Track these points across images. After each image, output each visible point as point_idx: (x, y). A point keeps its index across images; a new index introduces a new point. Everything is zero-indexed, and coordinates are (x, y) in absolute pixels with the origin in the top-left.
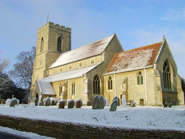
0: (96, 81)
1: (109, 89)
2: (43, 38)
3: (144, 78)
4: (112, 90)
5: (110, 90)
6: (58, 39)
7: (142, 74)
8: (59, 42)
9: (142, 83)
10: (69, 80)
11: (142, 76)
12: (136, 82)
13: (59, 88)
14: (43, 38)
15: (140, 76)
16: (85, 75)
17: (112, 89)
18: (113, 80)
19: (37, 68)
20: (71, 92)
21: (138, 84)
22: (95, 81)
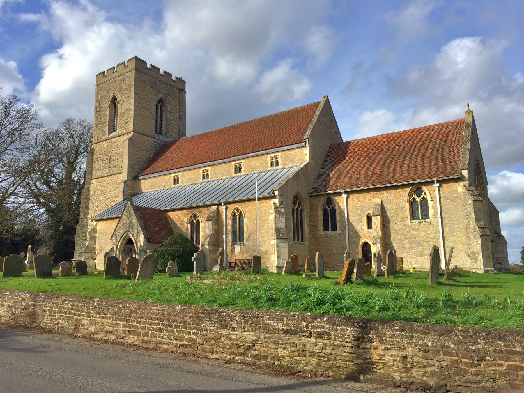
0: (297, 210)
1: (326, 229)
2: (114, 99)
3: (430, 204)
4: (334, 232)
5: (330, 232)
6: (157, 105)
7: (425, 194)
8: (159, 110)
9: (426, 216)
10: (223, 207)
11: (424, 198)
12: (408, 214)
13: (291, 211)
14: (114, 99)
15: (418, 199)
16: (276, 193)
17: (334, 228)
18: (428, 197)
19: (99, 173)
20: (230, 237)
21: (413, 216)
22: (295, 208)
